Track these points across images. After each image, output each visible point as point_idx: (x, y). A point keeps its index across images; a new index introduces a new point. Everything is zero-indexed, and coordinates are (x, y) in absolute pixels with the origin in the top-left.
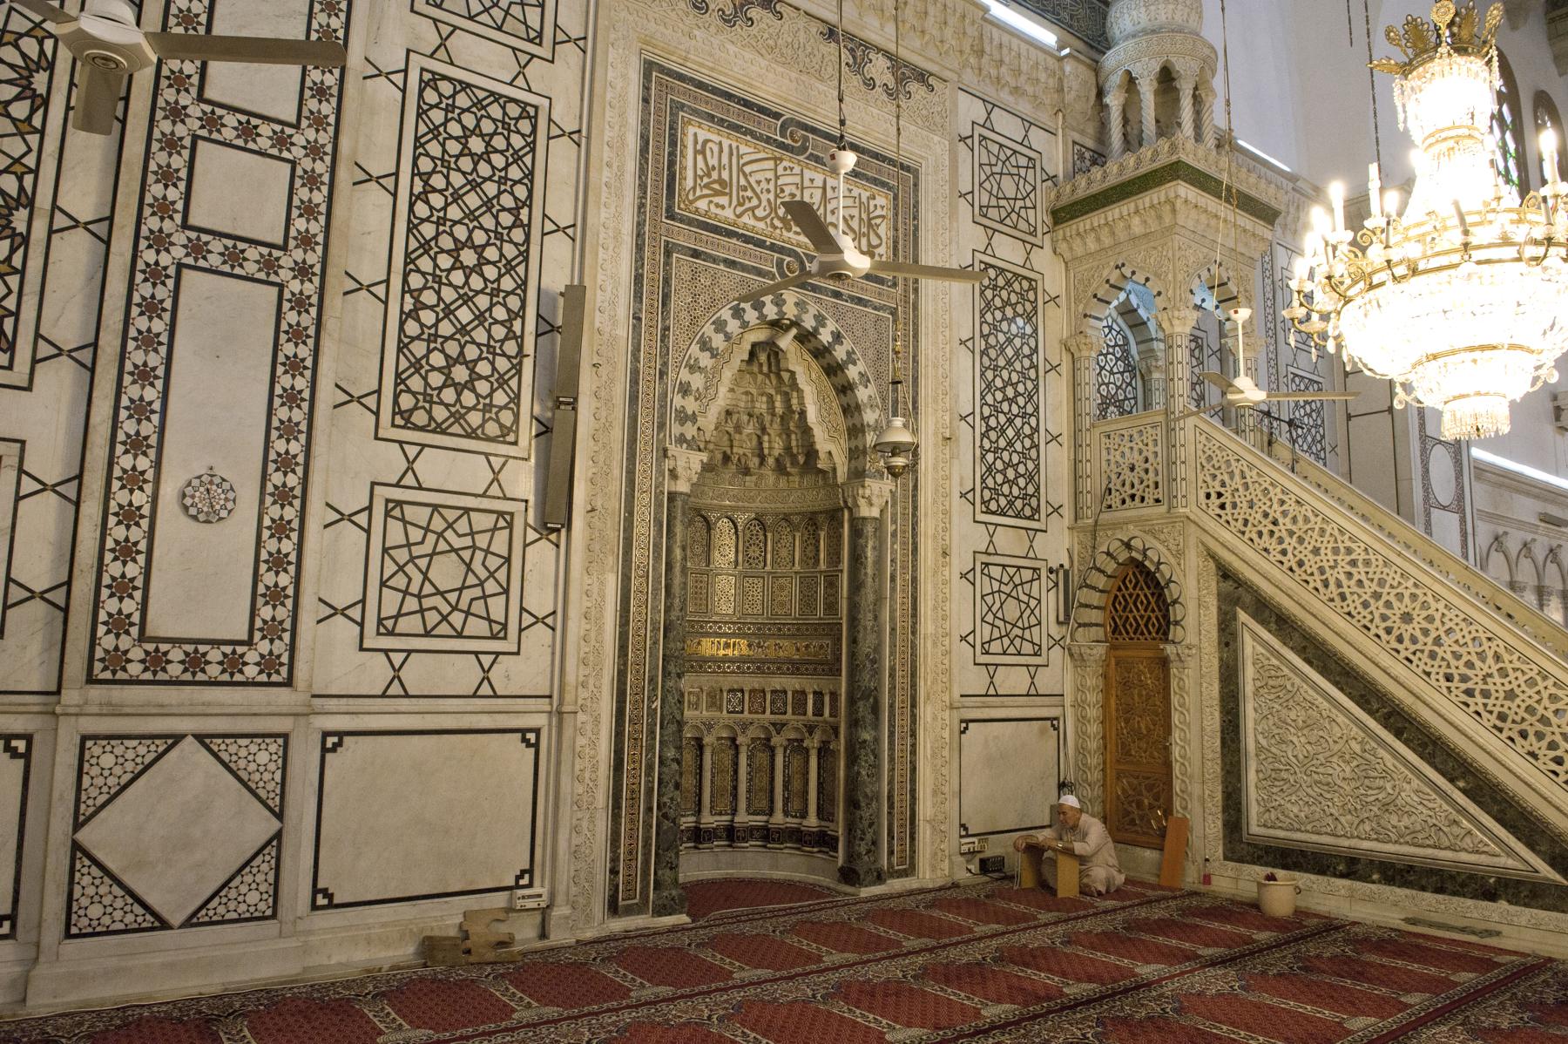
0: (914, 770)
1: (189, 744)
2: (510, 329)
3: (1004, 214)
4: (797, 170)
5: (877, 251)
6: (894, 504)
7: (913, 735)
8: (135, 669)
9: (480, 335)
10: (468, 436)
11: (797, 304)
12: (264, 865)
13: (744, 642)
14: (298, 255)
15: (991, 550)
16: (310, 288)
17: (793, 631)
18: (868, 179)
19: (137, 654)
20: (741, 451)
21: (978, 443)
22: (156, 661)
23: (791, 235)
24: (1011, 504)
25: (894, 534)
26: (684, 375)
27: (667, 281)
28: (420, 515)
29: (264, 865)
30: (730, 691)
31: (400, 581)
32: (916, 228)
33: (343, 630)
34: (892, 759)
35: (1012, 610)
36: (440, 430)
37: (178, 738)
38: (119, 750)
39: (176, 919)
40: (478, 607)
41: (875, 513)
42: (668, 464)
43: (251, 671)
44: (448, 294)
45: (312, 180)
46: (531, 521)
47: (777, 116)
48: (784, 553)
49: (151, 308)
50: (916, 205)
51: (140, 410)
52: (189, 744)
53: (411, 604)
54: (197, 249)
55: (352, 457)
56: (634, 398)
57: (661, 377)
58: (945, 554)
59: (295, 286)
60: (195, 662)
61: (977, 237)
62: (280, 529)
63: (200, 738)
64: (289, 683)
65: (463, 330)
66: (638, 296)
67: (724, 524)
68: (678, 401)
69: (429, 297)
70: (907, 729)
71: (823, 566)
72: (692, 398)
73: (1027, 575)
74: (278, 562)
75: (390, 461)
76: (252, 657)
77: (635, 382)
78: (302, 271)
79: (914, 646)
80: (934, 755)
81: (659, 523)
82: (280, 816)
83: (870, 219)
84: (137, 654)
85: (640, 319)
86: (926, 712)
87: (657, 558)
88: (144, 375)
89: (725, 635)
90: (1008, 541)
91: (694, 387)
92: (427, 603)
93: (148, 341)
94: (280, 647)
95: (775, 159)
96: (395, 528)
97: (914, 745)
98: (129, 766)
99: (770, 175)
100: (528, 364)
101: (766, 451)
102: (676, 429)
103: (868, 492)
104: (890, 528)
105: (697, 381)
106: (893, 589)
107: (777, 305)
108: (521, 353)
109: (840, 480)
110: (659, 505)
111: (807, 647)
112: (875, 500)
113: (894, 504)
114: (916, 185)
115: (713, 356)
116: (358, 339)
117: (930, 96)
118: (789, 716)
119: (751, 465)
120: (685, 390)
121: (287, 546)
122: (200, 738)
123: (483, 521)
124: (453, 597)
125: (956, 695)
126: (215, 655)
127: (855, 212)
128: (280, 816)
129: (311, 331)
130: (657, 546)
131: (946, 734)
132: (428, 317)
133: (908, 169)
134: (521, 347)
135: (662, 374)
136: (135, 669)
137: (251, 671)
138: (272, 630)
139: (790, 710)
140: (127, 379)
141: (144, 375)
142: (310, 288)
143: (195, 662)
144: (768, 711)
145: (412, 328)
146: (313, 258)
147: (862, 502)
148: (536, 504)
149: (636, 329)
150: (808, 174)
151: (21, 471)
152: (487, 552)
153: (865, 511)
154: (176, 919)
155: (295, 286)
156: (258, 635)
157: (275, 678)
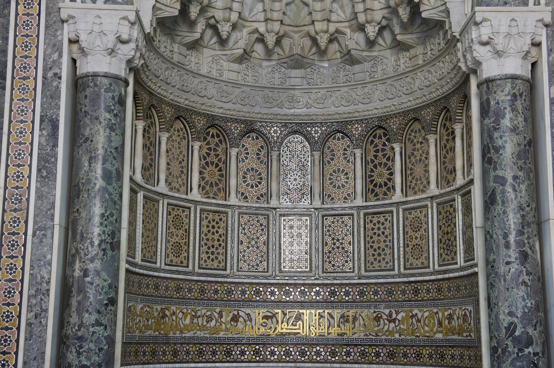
13: (367, 313)
17: (433, 294)
20: (332, 28)
41: (514, 66)
42: (67, 32)
48: (419, 170)
67: (339, 144)
71: (460, 181)
89: (341, 303)
101: (362, 18)
103: (485, 32)
109: (456, 29)
110: (51, 96)
111: (450, 318)
112: (500, 42)
119: (351, 45)
147: (481, 52)
153: (491, 68)
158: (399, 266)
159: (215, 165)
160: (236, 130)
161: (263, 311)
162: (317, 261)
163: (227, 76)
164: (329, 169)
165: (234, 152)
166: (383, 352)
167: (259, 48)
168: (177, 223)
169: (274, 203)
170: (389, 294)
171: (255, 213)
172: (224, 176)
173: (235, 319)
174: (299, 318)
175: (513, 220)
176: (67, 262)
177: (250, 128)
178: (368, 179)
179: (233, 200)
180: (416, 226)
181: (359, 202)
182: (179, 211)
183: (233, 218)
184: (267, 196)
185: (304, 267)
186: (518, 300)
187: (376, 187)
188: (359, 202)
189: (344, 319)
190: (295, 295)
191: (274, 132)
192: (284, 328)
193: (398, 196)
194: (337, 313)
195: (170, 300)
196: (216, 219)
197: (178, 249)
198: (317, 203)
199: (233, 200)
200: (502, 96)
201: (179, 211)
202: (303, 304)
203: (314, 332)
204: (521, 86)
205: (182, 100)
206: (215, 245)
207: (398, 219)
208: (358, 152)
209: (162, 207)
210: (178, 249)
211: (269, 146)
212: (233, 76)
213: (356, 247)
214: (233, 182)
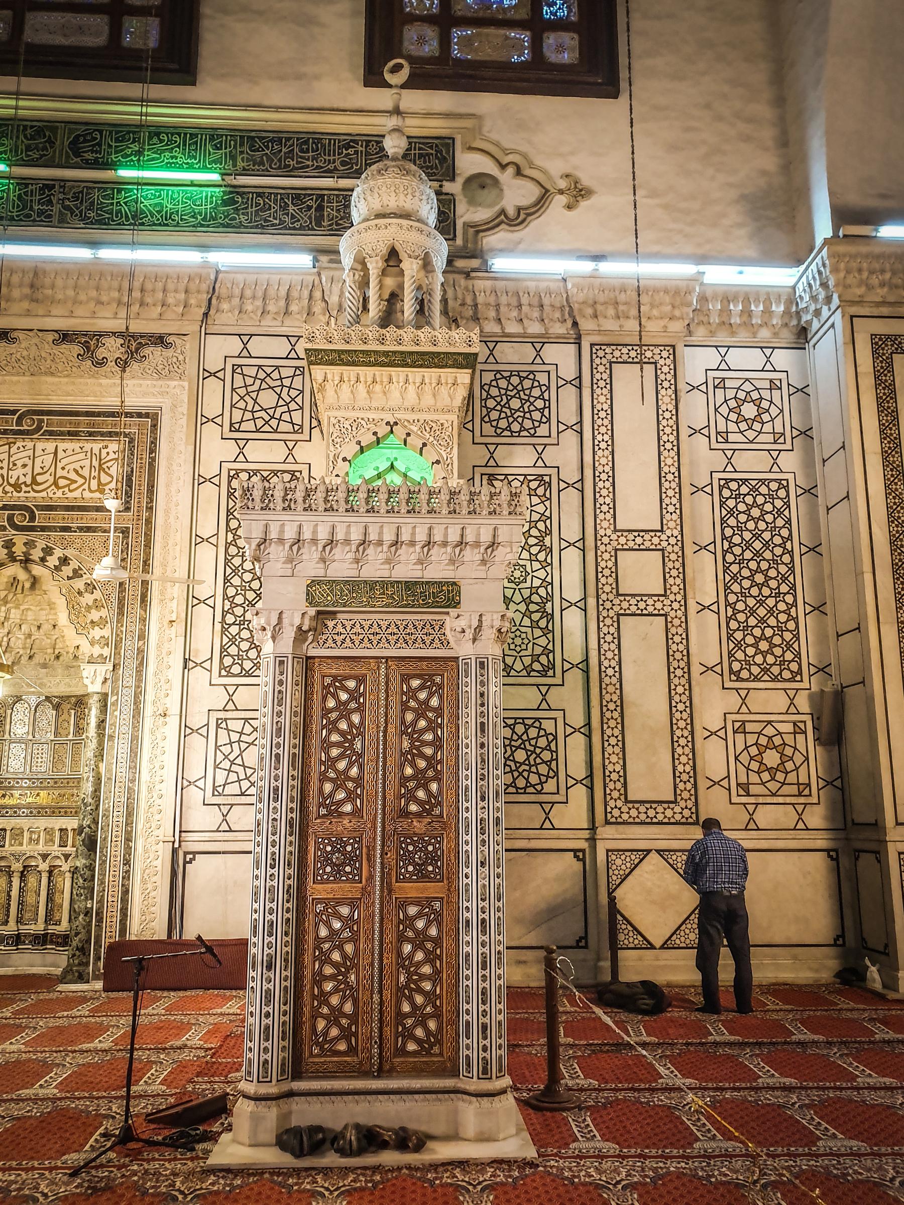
0: (126, 892)
3: (260, 423)
4: (30, 445)
5: (107, 488)
7: (127, 863)
11: (25, 544)
18: (102, 434)
21: (219, 618)
23: (22, 494)
25: (114, 704)
32: (154, 459)
47: (14, 412)
50: (153, 443)
61: (231, 450)
70: (120, 859)
80: (144, 881)
83: (100, 465)
86: (139, 845)
95: (9, 444)
99: (6, 456)
107: (7, 548)
114: (154, 426)
117: (169, 353)
118: (56, 847)
127: (87, 463)
131: (158, 863)
133: (147, 415)
150: (40, 446)
164: (60, 720)
174: (38, 795)
208: (73, 712)
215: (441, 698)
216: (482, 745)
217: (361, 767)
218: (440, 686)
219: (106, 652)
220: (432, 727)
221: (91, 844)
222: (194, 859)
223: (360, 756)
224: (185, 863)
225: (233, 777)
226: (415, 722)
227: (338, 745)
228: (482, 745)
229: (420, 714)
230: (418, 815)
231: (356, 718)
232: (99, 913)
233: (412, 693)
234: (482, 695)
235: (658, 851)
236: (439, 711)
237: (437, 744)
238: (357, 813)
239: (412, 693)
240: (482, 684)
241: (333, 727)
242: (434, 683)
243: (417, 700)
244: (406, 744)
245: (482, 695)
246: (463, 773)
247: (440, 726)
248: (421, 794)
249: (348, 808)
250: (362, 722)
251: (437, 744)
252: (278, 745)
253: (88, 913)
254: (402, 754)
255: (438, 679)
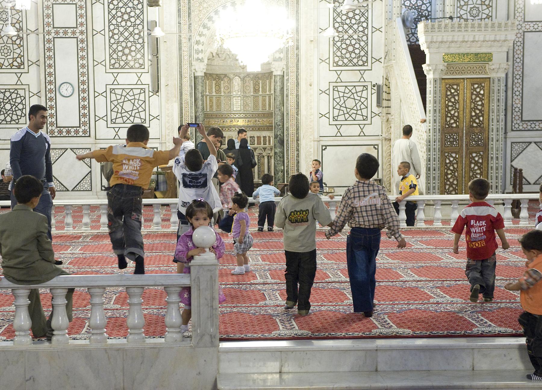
0: (298, 162)
1: (69, 150)
2: (140, 36)
6: (287, 69)
7: (298, 150)
8: (56, 134)
9: (131, 39)
10: (130, 68)
12: (88, 178)
14: (80, 28)
15: (339, 80)
16: (84, 37)
19: (56, 130)
22: (60, 132)
24: (351, 61)
25: (288, 80)
26: (198, 38)
27: (189, 9)
28: (119, 92)
29: (88, 178)
30: (250, 137)
31: (116, 110)
33: (101, 124)
34: (288, 158)
35: (350, 103)
36: (122, 68)
37: (67, 149)
38: (55, 152)
39: (70, 189)
40: (137, 115)
41: (279, 73)
43: (81, 134)
44: (121, 29)
45: (81, 7)
46: (150, 90)
48: (265, 87)
49: (49, 50)
51: (50, 74)
52: (69, 150)
53: (119, 115)
54: (57, 33)
55: (101, 78)
56: (180, 49)
57: (189, 40)
58: (311, 86)
59: (80, 37)
60: (68, 132)
62: (84, 99)
63: (71, 149)
64: (89, 136)
65: (126, 38)
66: (179, 16)
68: (196, 47)
69: (116, 31)
72: (201, 45)
73: (359, 89)
74: (84, 107)
75: (110, 78)
76: (81, 130)
77: (180, 43)
78: (82, 33)
79: (297, 119)
81: (191, 86)
82: (90, 167)
84: (56, 130)
85: (180, 23)
87: (191, 97)
88: (50, 66)
90: (350, 76)
91: (201, 41)
92: (123, 115)
93: (50, 58)
94: (87, 128)
96: (113, 96)
97: (298, 154)
98: (57, 155)
100: (146, 45)
102: (196, 56)
104: (285, 78)
105: (202, 39)
106: (287, 100)
108: (143, 42)
110: (191, 81)
113: (287, 69)
115: (208, 30)
116: (100, 48)
120: (198, 43)
121: (86, 103)
122: (71, 149)
123: (136, 92)
124: (130, 113)
125: (316, 136)
126: (72, 130)
128: (90, 167)
129: (86, 48)
130: (191, 94)
131: (312, 150)
132: (116, 37)
134: (143, 40)
135: (189, 39)
136: (56, 134)
137: (81, 134)
138: (85, 124)
139: (267, 143)
140: (47, 68)
141: (50, 66)
142: (84, 37)
143: (68, 132)
144: (262, 143)
145: (112, 41)
146: (84, 28)
148: (152, 85)
149: (180, 27)
151: (29, 91)
152: (139, 100)
154: (70, 189)
155: (80, 37)
156: (81, 125)
157: (86, 135)
158: (260, 109)
159: (218, 86)
160: (222, 76)
161: (230, 120)
162: (242, 108)
163: (220, 64)
164: (245, 85)
165: (222, 82)
166: (257, 128)
167: (228, 56)
168: (211, 101)
169: (232, 94)
170: (259, 116)
171: (228, 97)
172: (220, 88)
173: (224, 122)
175: (278, 103)
176: (196, 112)
177: (226, 75)
178: (254, 88)
179: (222, 94)
180: (264, 100)
181: (252, 94)
182: (211, 97)
183: (222, 98)
184: (230, 92)
185: (239, 109)
186: (279, 118)
187: (256, 90)
188: (252, 94)
189: (249, 121)
190: (237, 116)
191: (231, 76)
192: (234, 123)
193: (261, 93)
194: (247, 120)
195: (209, 118)
196: (219, 98)
197: (211, 107)
198: (242, 94)
199: (222, 94)
200: (278, 79)
201: (211, 97)
202: (239, 118)
203: (242, 124)
204: (281, 77)
205: (211, 72)
206: (219, 105)
207: (260, 98)
209: (208, 98)
210: (211, 107)
211: (230, 80)
212: (222, 64)
213: (251, 105)
214: (222, 90)
215: (484, 90)
216: (498, 106)
217: (458, 113)
218: (484, 87)
219: (282, 56)
220: (481, 100)
221: (282, 142)
222: (326, 148)
223: (458, 109)
224: (322, 150)
225: (341, 113)
226: (475, 99)
227: (451, 106)
228: (498, 106)
229: (477, 96)
230: (476, 127)
231: (457, 98)
232: (287, 171)
233: (475, 89)
234: (499, 90)
235: (535, 143)
236: (483, 95)
237: (482, 105)
238: (457, 126)
239: (475, 89)
240: (499, 86)
241: (449, 101)
242: (482, 86)
243: (476, 91)
244: (472, 106)
245: (499, 90)
246: (491, 114)
247: (484, 100)
248: (477, 121)
249: (454, 125)
250: (459, 99)
251: (482, 105)
252: (435, 107)
253: (283, 171)
254: (471, 108)
255: (483, 84)
